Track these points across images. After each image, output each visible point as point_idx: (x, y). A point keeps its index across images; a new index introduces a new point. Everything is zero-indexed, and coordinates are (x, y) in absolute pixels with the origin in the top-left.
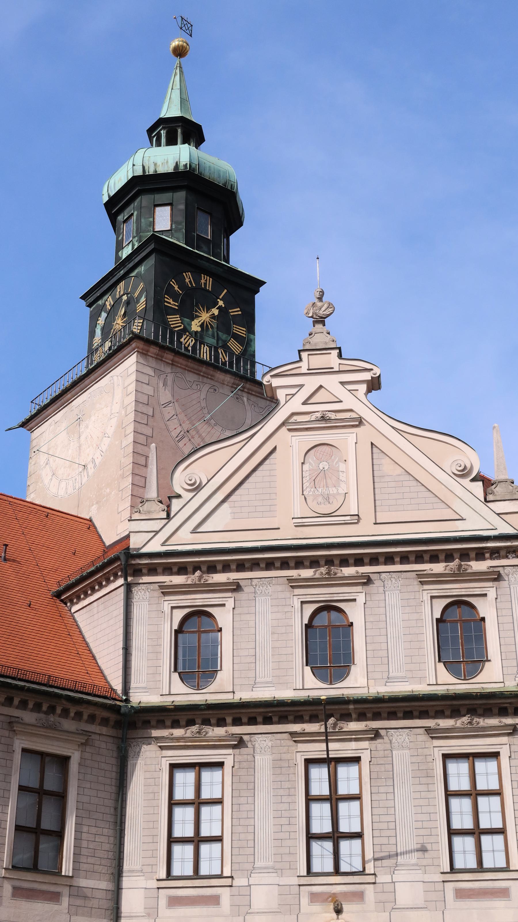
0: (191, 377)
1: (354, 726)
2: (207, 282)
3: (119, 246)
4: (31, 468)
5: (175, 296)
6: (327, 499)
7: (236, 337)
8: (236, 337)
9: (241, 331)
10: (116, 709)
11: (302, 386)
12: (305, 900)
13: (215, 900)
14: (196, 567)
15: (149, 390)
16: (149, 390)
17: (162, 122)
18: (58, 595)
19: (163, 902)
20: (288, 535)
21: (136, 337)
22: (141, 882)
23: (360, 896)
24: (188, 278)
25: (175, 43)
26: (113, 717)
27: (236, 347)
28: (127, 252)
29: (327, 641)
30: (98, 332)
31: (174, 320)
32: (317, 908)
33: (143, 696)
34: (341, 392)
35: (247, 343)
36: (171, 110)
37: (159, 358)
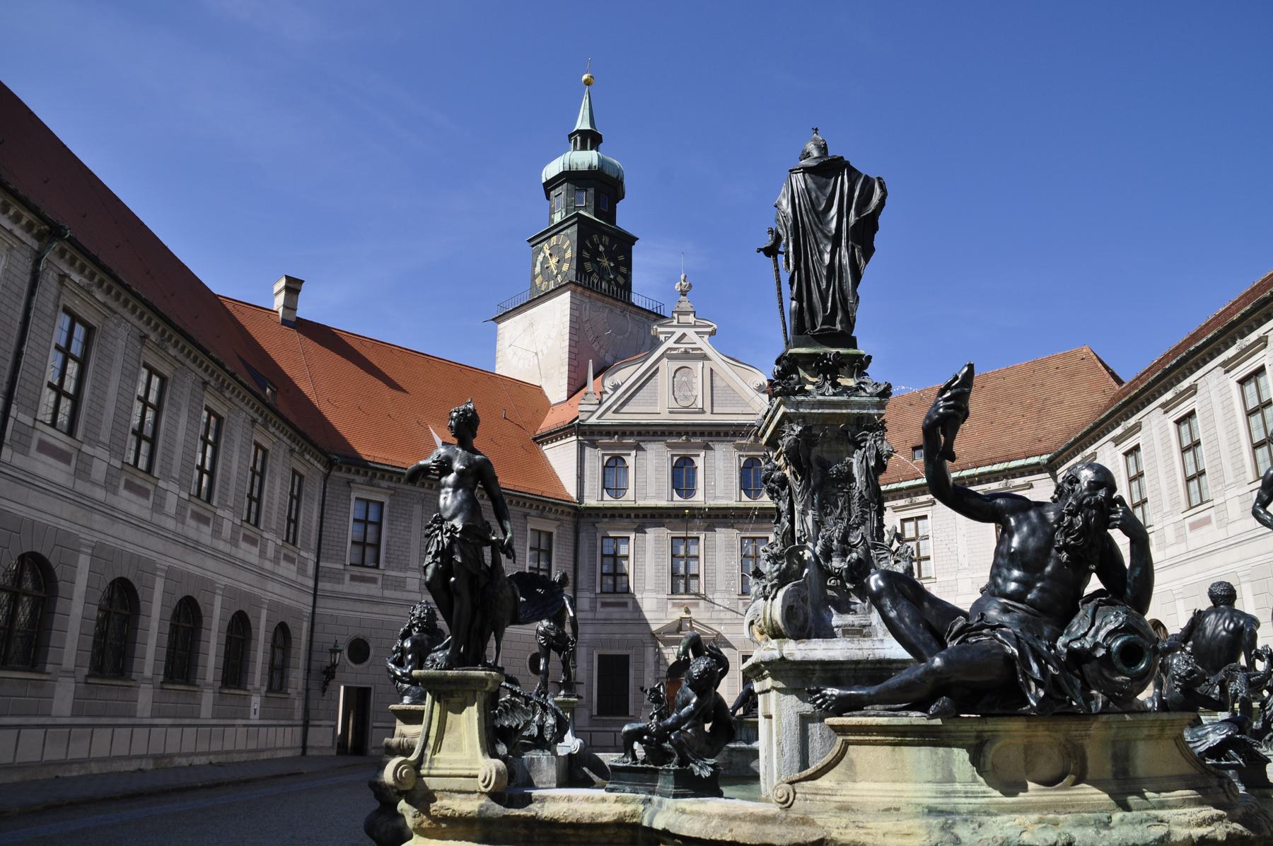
0: (600, 304)
1: (697, 521)
2: (606, 239)
3: (552, 212)
4: (498, 347)
5: (588, 250)
6: (686, 397)
7: (622, 274)
8: (622, 274)
9: (623, 270)
10: (576, 508)
11: (673, 333)
12: (670, 606)
13: (625, 605)
14: (616, 433)
15: (577, 313)
16: (577, 313)
17: (578, 131)
18: (535, 439)
19: (599, 605)
20: (664, 417)
21: (571, 282)
22: (588, 594)
23: (697, 605)
24: (595, 238)
25: (585, 77)
26: (572, 511)
27: (621, 280)
28: (557, 218)
29: (682, 476)
30: (538, 264)
31: (588, 266)
32: (675, 609)
33: (591, 501)
34: (695, 338)
35: (628, 277)
36: (583, 124)
37: (582, 294)
